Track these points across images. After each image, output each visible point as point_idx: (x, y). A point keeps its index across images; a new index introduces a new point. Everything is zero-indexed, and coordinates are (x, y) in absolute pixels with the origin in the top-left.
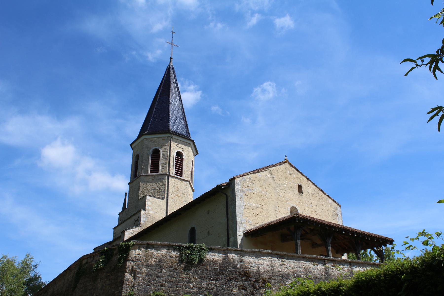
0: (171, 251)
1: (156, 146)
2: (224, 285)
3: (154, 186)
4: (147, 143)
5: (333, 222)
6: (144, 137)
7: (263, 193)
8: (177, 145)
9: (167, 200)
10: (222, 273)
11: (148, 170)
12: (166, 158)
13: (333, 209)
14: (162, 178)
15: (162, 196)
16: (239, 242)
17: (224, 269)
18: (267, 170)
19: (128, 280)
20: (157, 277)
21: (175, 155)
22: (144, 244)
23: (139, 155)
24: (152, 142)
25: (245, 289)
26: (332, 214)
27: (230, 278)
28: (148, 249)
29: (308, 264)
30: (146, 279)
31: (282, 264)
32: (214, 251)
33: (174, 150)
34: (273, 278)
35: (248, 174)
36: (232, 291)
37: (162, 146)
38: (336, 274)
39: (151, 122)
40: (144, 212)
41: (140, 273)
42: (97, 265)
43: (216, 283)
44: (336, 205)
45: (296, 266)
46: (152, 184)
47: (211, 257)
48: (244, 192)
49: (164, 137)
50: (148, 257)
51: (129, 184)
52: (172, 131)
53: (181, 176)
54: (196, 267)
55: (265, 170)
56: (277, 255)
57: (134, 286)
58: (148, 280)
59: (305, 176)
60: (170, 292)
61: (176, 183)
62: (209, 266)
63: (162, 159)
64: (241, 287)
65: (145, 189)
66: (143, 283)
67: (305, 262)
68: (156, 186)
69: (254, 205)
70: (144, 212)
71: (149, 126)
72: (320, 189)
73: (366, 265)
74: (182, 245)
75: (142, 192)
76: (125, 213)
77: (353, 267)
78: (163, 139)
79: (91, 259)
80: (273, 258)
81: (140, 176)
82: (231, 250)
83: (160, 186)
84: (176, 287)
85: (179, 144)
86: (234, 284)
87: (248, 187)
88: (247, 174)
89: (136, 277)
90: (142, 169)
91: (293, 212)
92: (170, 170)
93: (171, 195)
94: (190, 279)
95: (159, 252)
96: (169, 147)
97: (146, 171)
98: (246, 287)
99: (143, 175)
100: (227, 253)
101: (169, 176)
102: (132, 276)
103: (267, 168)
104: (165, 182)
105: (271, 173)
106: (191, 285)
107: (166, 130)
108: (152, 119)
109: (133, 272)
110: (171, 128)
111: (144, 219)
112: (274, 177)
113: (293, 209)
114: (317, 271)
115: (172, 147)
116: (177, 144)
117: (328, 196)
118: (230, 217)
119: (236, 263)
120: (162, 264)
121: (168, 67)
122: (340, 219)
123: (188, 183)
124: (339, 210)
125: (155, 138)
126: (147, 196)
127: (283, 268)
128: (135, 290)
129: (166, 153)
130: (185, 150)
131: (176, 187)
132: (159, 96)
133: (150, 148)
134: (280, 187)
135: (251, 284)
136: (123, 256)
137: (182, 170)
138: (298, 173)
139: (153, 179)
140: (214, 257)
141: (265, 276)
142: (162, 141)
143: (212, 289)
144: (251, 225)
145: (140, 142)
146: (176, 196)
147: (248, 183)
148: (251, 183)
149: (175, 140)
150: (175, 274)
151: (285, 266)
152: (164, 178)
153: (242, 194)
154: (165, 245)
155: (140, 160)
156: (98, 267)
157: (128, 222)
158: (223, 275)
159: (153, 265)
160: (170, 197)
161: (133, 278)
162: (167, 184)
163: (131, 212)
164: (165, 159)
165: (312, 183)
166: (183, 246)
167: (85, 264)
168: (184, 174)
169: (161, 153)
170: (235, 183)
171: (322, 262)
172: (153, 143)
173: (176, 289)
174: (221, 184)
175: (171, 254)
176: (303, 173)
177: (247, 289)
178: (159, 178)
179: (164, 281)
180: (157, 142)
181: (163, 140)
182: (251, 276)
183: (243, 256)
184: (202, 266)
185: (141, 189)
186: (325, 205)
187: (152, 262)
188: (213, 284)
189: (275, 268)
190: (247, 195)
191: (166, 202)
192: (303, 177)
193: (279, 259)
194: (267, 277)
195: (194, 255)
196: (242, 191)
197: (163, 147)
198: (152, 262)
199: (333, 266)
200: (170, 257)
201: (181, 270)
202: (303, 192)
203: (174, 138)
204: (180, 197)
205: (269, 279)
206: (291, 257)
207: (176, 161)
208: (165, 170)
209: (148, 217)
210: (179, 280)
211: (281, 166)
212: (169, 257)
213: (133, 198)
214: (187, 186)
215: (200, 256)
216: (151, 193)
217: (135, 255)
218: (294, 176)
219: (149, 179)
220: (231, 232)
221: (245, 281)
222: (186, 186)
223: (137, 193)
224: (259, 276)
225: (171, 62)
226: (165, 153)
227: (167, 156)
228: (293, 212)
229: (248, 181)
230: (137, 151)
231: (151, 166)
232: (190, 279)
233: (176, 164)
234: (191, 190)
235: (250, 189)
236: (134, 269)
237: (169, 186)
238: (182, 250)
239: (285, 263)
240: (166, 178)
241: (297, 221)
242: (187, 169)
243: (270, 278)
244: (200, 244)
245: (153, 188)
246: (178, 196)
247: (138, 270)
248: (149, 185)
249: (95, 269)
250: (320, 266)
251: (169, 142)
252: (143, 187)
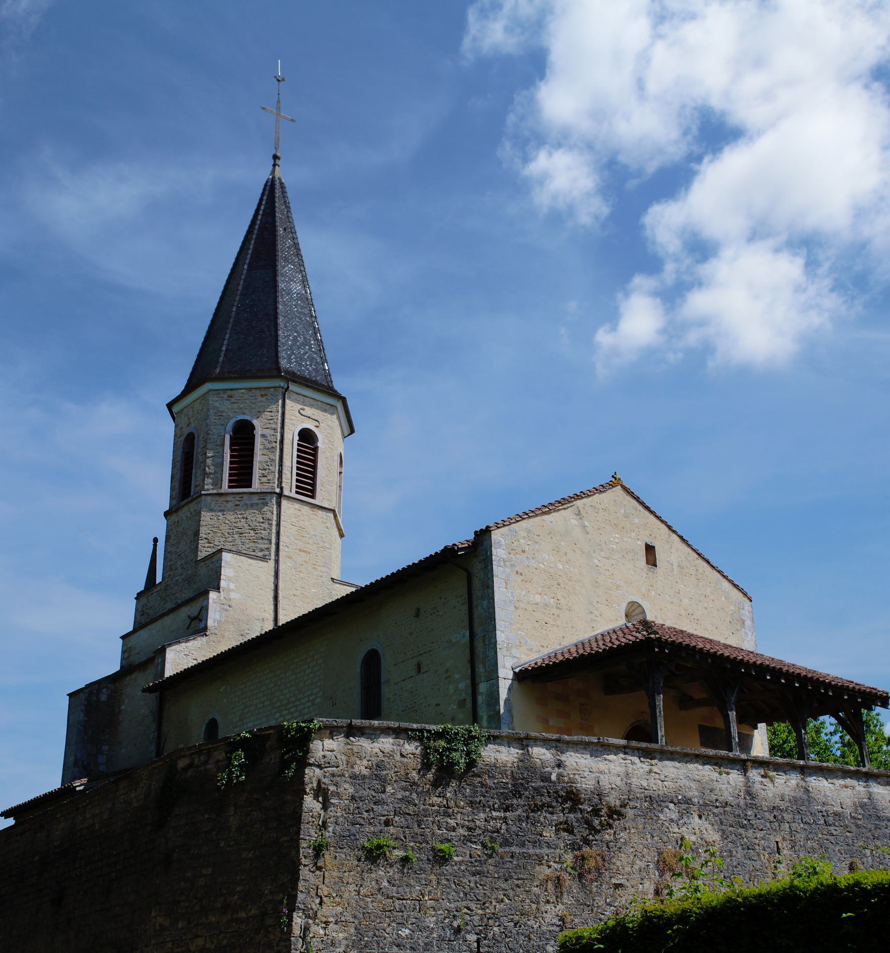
0: (402, 741)
1: (244, 414)
2: (523, 821)
3: (239, 525)
4: (217, 404)
5: (733, 642)
6: (208, 386)
7: (561, 567)
8: (301, 411)
9: (275, 563)
10: (517, 794)
11: (222, 480)
12: (273, 448)
13: (732, 608)
14: (262, 501)
15: (262, 550)
16: (503, 694)
17: (522, 784)
18: (568, 507)
19: (311, 811)
20: (375, 803)
21: (297, 438)
22: (342, 727)
23: (196, 437)
24: (233, 400)
25: (570, 831)
26: (729, 619)
27: (536, 805)
28: (351, 738)
29: (707, 772)
30: (351, 809)
31: (650, 771)
32: (498, 741)
33: (292, 424)
34: (631, 803)
35: (524, 519)
36: (541, 835)
37: (259, 412)
38: (771, 795)
39: (226, 342)
40: (215, 597)
41: (338, 795)
42: (228, 775)
43: (505, 818)
44: (741, 595)
45: (682, 777)
46: (233, 517)
47: (493, 755)
48: (513, 566)
49: (266, 388)
50: (351, 754)
51: (167, 514)
52: (287, 372)
53: (313, 497)
54: (461, 778)
55: (565, 506)
56: (638, 749)
57: (324, 825)
58: (356, 811)
59: (662, 521)
60: (405, 837)
61: (298, 516)
62: (489, 776)
63: (260, 449)
64: (562, 827)
65: (215, 533)
66: (345, 818)
67: (700, 767)
68: (245, 525)
69: (538, 598)
70: (215, 597)
71: (223, 354)
72: (699, 554)
73: (840, 774)
74: (427, 727)
75: (206, 539)
76: (155, 594)
77: (808, 779)
78: (263, 393)
79: (203, 758)
80: (630, 757)
81: (201, 495)
82: (536, 739)
83: (258, 524)
84: (419, 826)
85: (305, 407)
86: (545, 817)
87: (524, 551)
88: (521, 518)
89: (327, 803)
90: (205, 475)
91: (633, 614)
92: (284, 480)
93: (286, 549)
94: (448, 807)
95: (375, 744)
96: (280, 415)
97: (218, 483)
98: (572, 827)
99: (209, 492)
100: (528, 746)
101: (280, 495)
102: (318, 801)
103: (569, 502)
104: (269, 513)
105: (579, 514)
106: (452, 822)
107: (273, 370)
108: (231, 334)
109: (321, 792)
110: (283, 363)
111: (217, 617)
112: (587, 524)
113: (634, 608)
114: (727, 789)
115: (287, 416)
117: (719, 572)
118: (478, 630)
119: (547, 769)
120: (385, 772)
121: (267, 182)
122: (750, 633)
123: (331, 515)
124: (746, 607)
125: (240, 391)
126: (223, 553)
127: (653, 781)
128: (328, 834)
129: (272, 432)
130: (321, 424)
131: (300, 527)
132: (246, 267)
133: (228, 419)
134: (602, 550)
135: (582, 818)
136: (296, 754)
137: (314, 479)
138: (647, 513)
139: (238, 503)
140: (498, 756)
141: (613, 800)
142: (260, 399)
143: (498, 832)
144: (531, 650)
145: (198, 399)
146: (300, 550)
147: (522, 541)
148: (529, 543)
149: (296, 396)
150: (414, 796)
151: (657, 776)
152: (268, 501)
153: (508, 570)
154: (389, 728)
155: (198, 449)
156: (230, 779)
157: (168, 620)
158: (520, 797)
159: (364, 777)
160: (285, 554)
161: (321, 806)
162: (275, 518)
163: (174, 594)
164: (268, 449)
165: (681, 537)
166: (429, 731)
167: (185, 769)
168: (321, 490)
169: (258, 432)
170: (493, 541)
171: (738, 767)
172: (233, 403)
173: (419, 831)
174: (454, 545)
175: (403, 750)
176: (658, 514)
177: (575, 831)
178: (252, 502)
179: (392, 813)
180: (245, 402)
181: (262, 396)
182: (582, 800)
183: (562, 753)
184: (473, 776)
185: (203, 532)
186: (712, 597)
187: (361, 768)
188: (500, 818)
189: (635, 781)
190: (521, 574)
191: (275, 568)
192: (659, 522)
193: (642, 759)
194: (618, 803)
195: (456, 750)
196: (508, 564)
197: (263, 416)
198: (361, 768)
199: (763, 776)
200: (402, 755)
201: (428, 786)
202: (658, 564)
204: (311, 555)
205: (621, 806)
206: (669, 756)
207: (297, 455)
208: (270, 480)
209: (226, 610)
210: (424, 810)
211: (603, 495)
212: (398, 757)
213: (180, 555)
214: (328, 525)
215: (468, 754)
216: (231, 544)
217: (322, 753)
218: (636, 521)
219: (225, 503)
220: (480, 669)
221: (569, 813)
222: (325, 523)
223: (191, 542)
224: (600, 800)
225: (277, 167)
226: (268, 432)
227: (276, 442)
228: (633, 614)
229: (524, 538)
230: (188, 425)
231: (229, 467)
232: (448, 807)
233: (298, 462)
234: (336, 533)
235: (527, 557)
236: (323, 786)
237: (282, 523)
238: (428, 739)
239: (655, 769)
240: (274, 501)
241: (656, 650)
242: (327, 476)
243: (624, 805)
244: (467, 726)
245: (238, 530)
246: (304, 551)
247: (332, 788)
248: (227, 522)
249: (223, 784)
250: (735, 776)
252: (209, 527)
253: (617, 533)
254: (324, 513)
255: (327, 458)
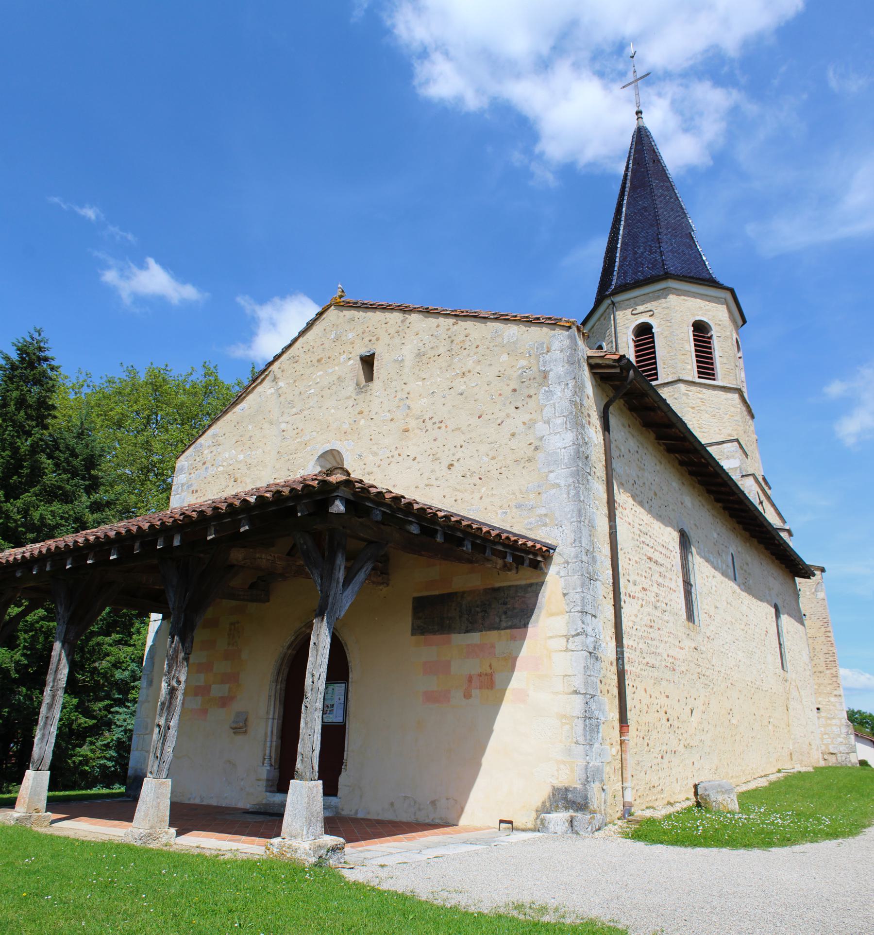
8: (634, 312)
116: (631, 310)
130: (655, 311)
149: (627, 303)
203: (623, 301)
214: (675, 396)
242: (668, 353)
251: (612, 316)
253: (319, 371)
254: (670, 387)
255: (666, 337)
